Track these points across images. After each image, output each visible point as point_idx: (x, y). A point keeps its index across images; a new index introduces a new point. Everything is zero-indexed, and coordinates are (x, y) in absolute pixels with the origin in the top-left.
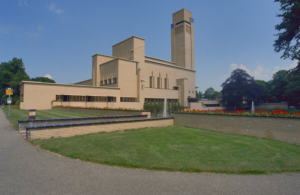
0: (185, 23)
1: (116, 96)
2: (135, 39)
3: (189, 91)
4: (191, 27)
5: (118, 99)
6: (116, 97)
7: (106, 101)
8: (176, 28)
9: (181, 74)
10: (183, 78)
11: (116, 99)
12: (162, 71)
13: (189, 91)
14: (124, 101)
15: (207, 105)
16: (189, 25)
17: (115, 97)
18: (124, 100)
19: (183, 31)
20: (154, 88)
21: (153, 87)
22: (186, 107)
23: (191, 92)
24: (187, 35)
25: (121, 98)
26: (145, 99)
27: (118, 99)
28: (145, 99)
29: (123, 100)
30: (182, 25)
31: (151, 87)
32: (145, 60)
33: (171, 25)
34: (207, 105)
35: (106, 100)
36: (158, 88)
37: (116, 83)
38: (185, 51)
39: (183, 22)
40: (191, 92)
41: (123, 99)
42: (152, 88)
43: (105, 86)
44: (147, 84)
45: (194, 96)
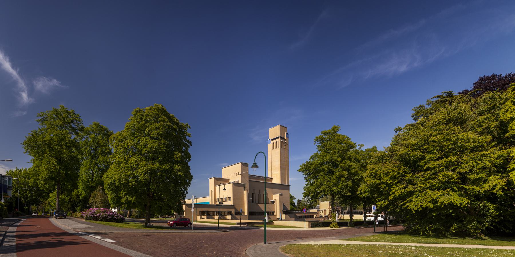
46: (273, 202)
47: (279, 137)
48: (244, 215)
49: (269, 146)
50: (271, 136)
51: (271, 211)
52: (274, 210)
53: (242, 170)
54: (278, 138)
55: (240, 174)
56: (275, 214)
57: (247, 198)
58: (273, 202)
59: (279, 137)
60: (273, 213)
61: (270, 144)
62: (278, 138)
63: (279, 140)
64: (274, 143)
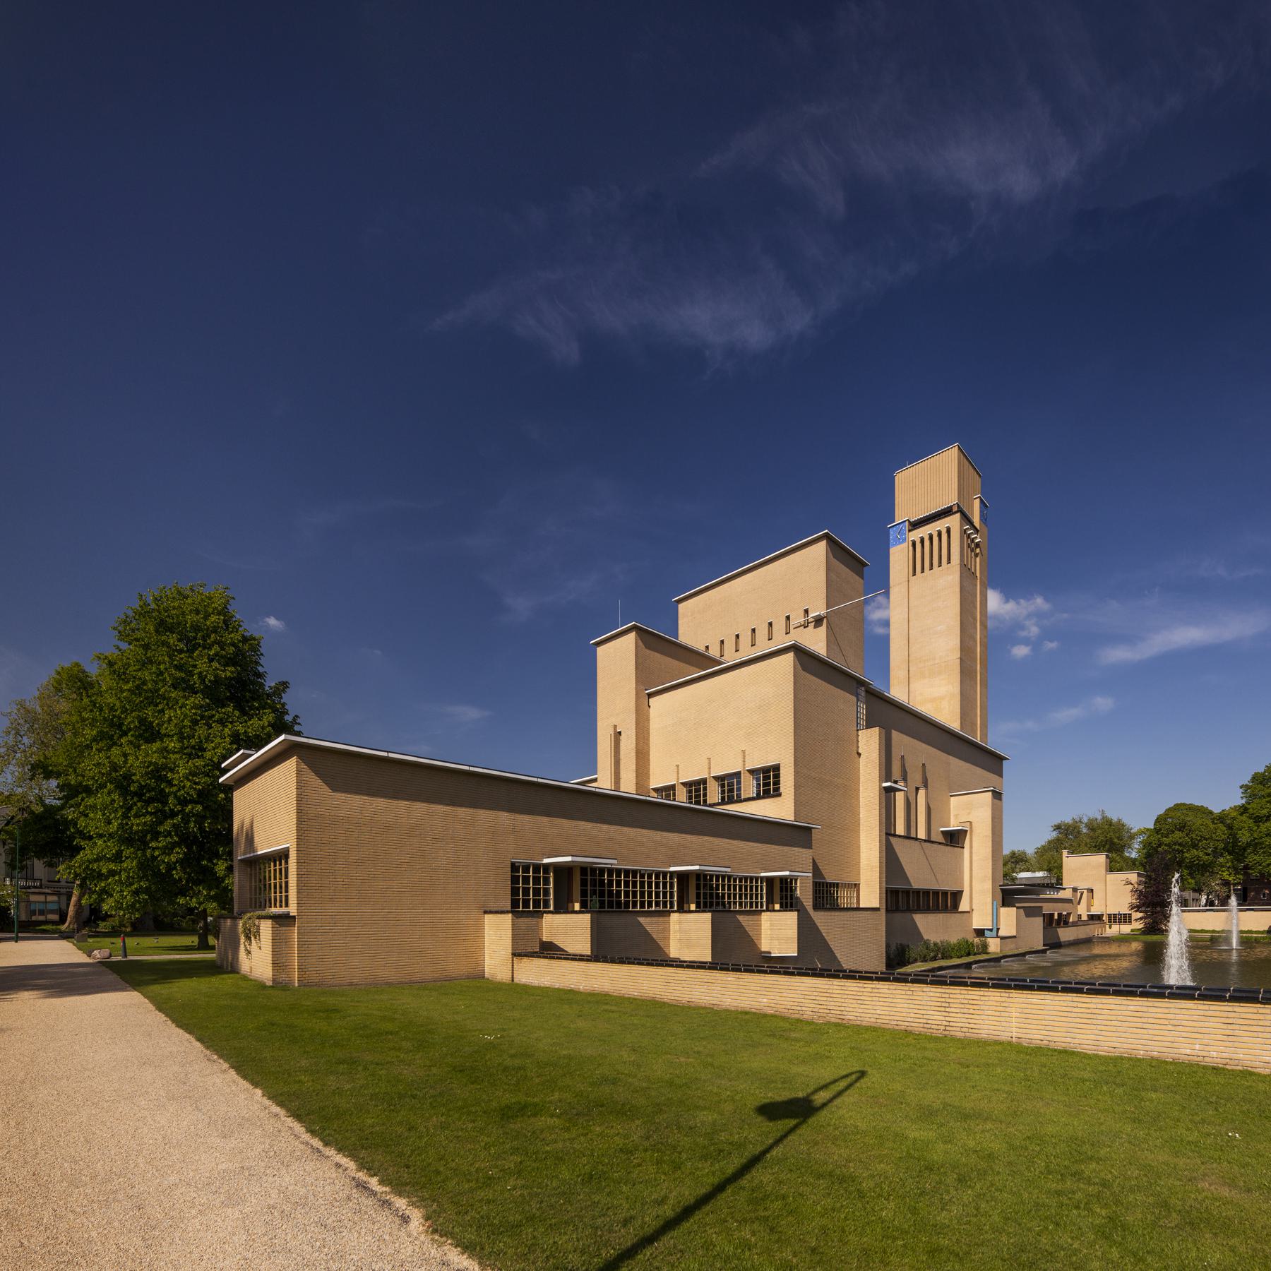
37: (780, 795)
46: (955, 838)
47: (955, 509)
48: (858, 909)
49: (899, 556)
50: (905, 508)
51: (936, 887)
52: (963, 887)
53: (834, 592)
54: (946, 512)
55: (818, 621)
56: (964, 906)
57: (881, 782)
58: (955, 838)
59: (955, 509)
60: (957, 895)
61: (905, 545)
62: (946, 512)
63: (954, 521)
64: (927, 543)
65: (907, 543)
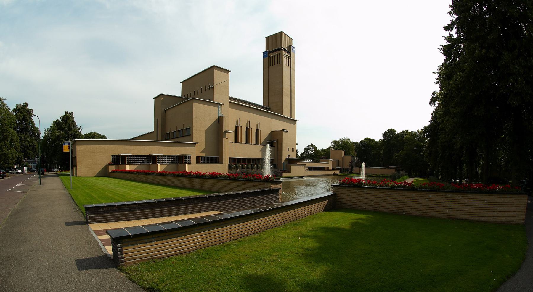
0: (284, 53)
1: (190, 155)
2: (216, 72)
3: (288, 149)
4: (290, 58)
5: (194, 160)
6: (190, 157)
7: (176, 162)
8: (270, 57)
9: (277, 125)
10: (281, 129)
11: (190, 159)
12: (255, 119)
13: (288, 149)
14: (202, 163)
15: (311, 169)
16: (289, 55)
17: (189, 156)
18: (202, 161)
19: (280, 62)
20: (241, 143)
21: (240, 142)
22: (285, 171)
23: (291, 150)
24: (286, 69)
25: (197, 157)
26: (230, 158)
27: (194, 160)
28: (230, 158)
29: (200, 160)
30: (280, 54)
31: (237, 141)
32: (230, 102)
33: (264, 52)
34: (311, 169)
35: (176, 160)
36: (247, 142)
38: (283, 91)
39: (280, 49)
40: (291, 150)
41: (200, 158)
42: (239, 143)
43: (173, 140)
44: (231, 137)
45: (293, 155)
65: (268, 57)
